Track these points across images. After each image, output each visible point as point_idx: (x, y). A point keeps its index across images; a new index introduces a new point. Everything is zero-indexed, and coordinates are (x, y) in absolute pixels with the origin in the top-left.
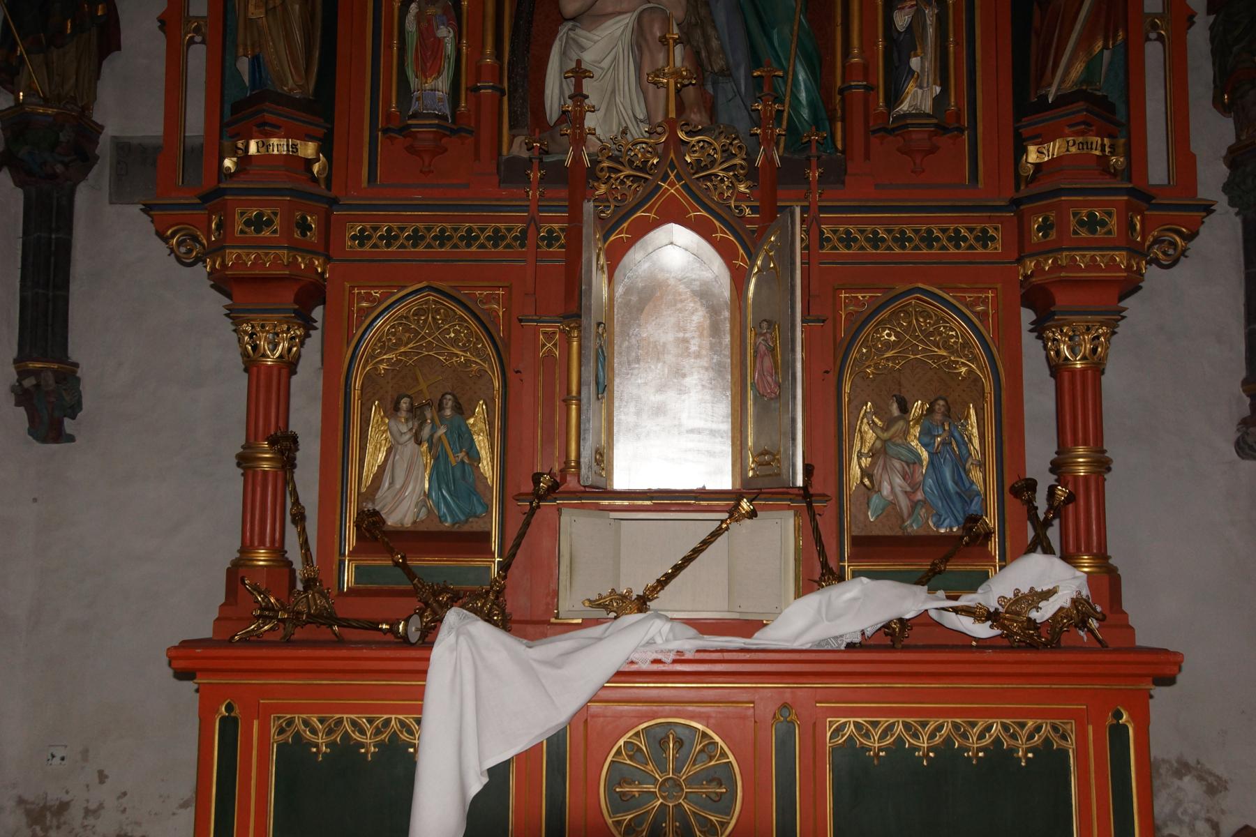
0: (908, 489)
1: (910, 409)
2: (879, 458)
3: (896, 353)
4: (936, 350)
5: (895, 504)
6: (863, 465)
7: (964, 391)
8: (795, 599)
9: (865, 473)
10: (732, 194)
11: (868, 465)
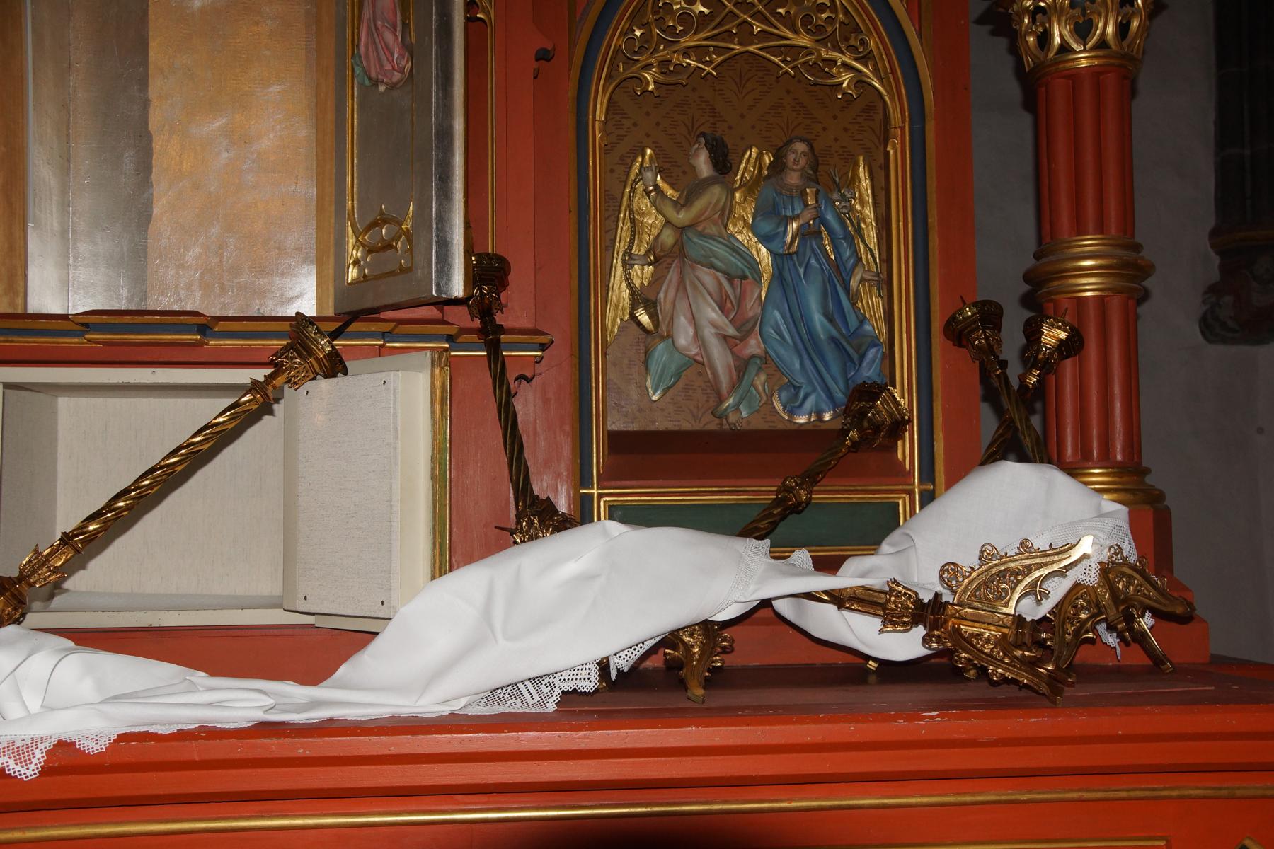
0: (731, 331)
1: (734, 168)
2: (668, 269)
3: (705, 39)
4: (790, 35)
5: (703, 364)
6: (637, 283)
7: (846, 130)
8: (433, 578)
9: (641, 298)
11: (646, 284)
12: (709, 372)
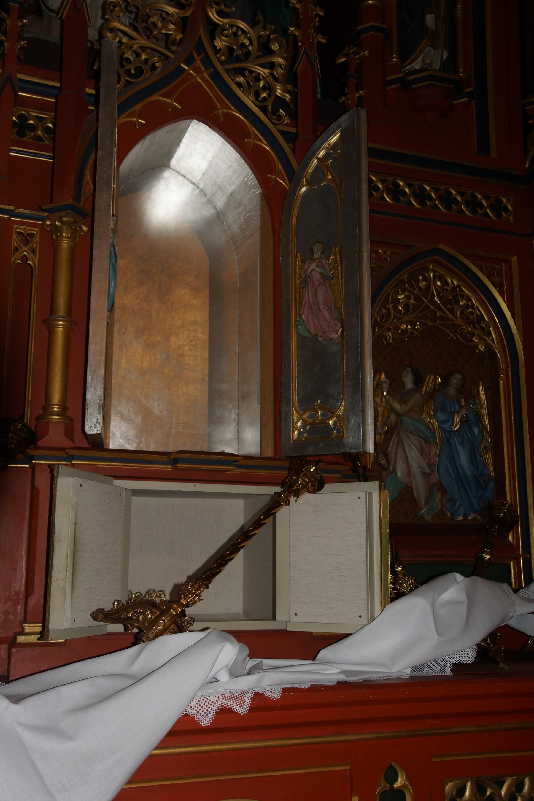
10: (269, 95)
12: (415, 491)
